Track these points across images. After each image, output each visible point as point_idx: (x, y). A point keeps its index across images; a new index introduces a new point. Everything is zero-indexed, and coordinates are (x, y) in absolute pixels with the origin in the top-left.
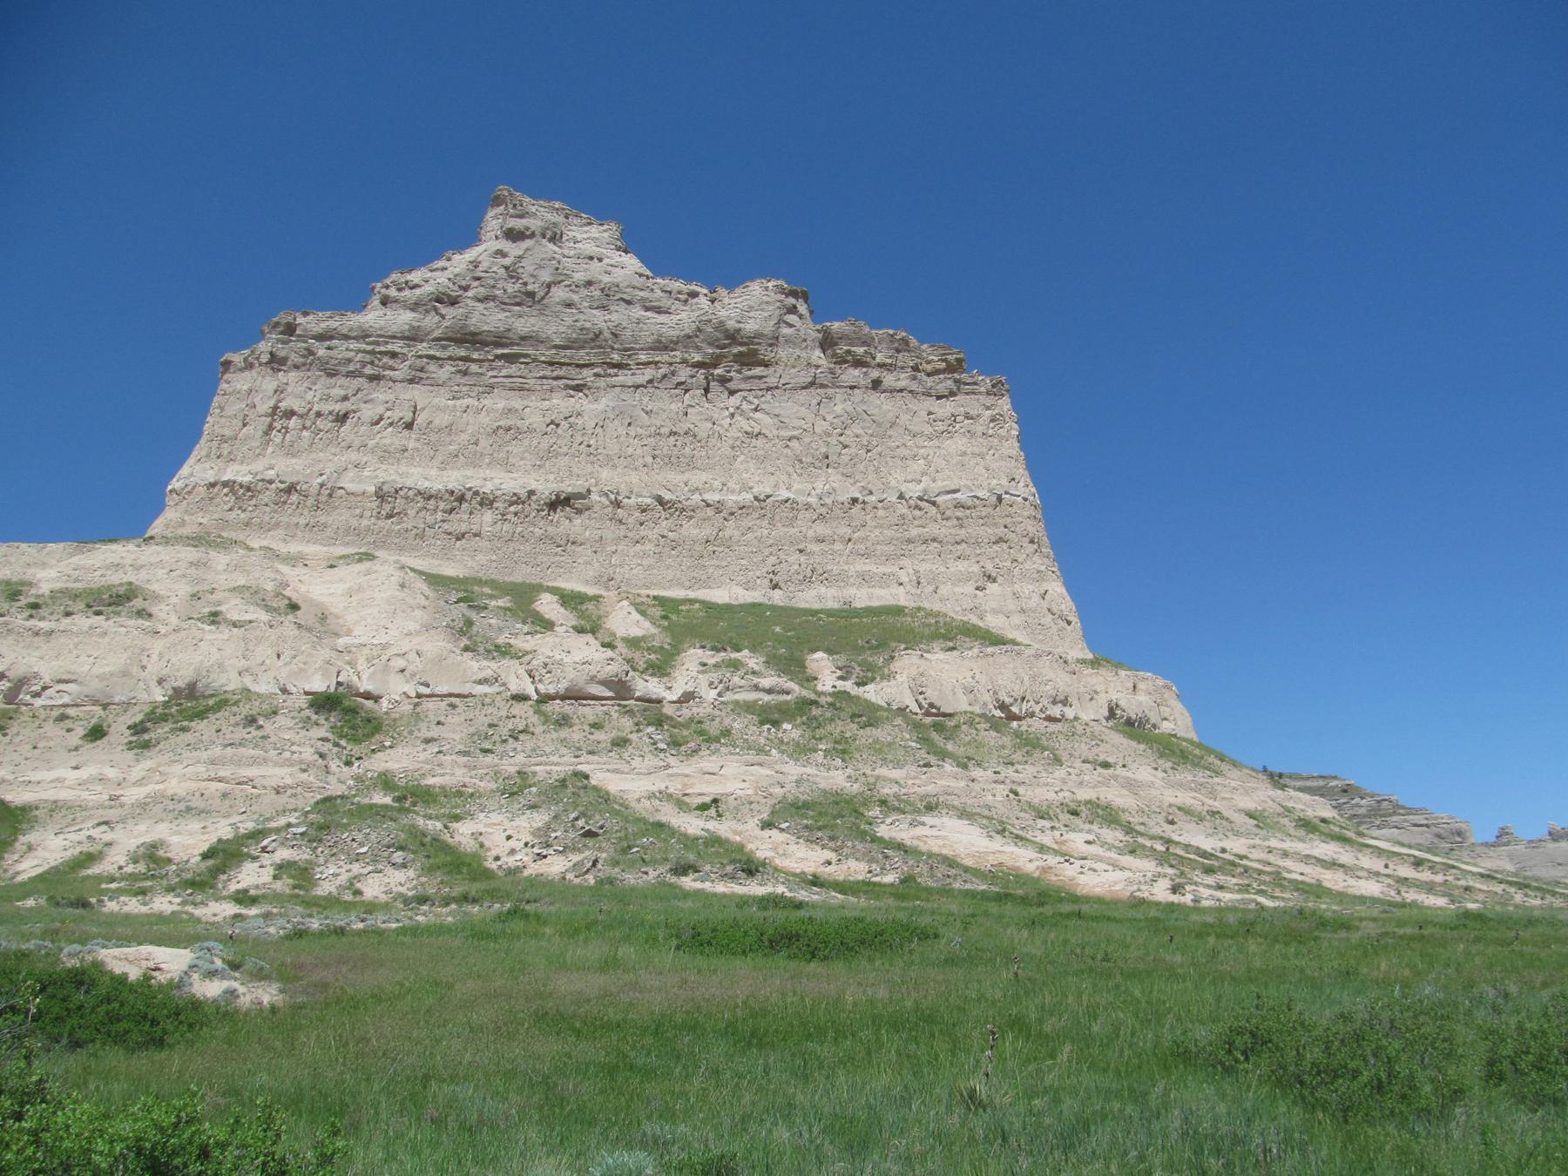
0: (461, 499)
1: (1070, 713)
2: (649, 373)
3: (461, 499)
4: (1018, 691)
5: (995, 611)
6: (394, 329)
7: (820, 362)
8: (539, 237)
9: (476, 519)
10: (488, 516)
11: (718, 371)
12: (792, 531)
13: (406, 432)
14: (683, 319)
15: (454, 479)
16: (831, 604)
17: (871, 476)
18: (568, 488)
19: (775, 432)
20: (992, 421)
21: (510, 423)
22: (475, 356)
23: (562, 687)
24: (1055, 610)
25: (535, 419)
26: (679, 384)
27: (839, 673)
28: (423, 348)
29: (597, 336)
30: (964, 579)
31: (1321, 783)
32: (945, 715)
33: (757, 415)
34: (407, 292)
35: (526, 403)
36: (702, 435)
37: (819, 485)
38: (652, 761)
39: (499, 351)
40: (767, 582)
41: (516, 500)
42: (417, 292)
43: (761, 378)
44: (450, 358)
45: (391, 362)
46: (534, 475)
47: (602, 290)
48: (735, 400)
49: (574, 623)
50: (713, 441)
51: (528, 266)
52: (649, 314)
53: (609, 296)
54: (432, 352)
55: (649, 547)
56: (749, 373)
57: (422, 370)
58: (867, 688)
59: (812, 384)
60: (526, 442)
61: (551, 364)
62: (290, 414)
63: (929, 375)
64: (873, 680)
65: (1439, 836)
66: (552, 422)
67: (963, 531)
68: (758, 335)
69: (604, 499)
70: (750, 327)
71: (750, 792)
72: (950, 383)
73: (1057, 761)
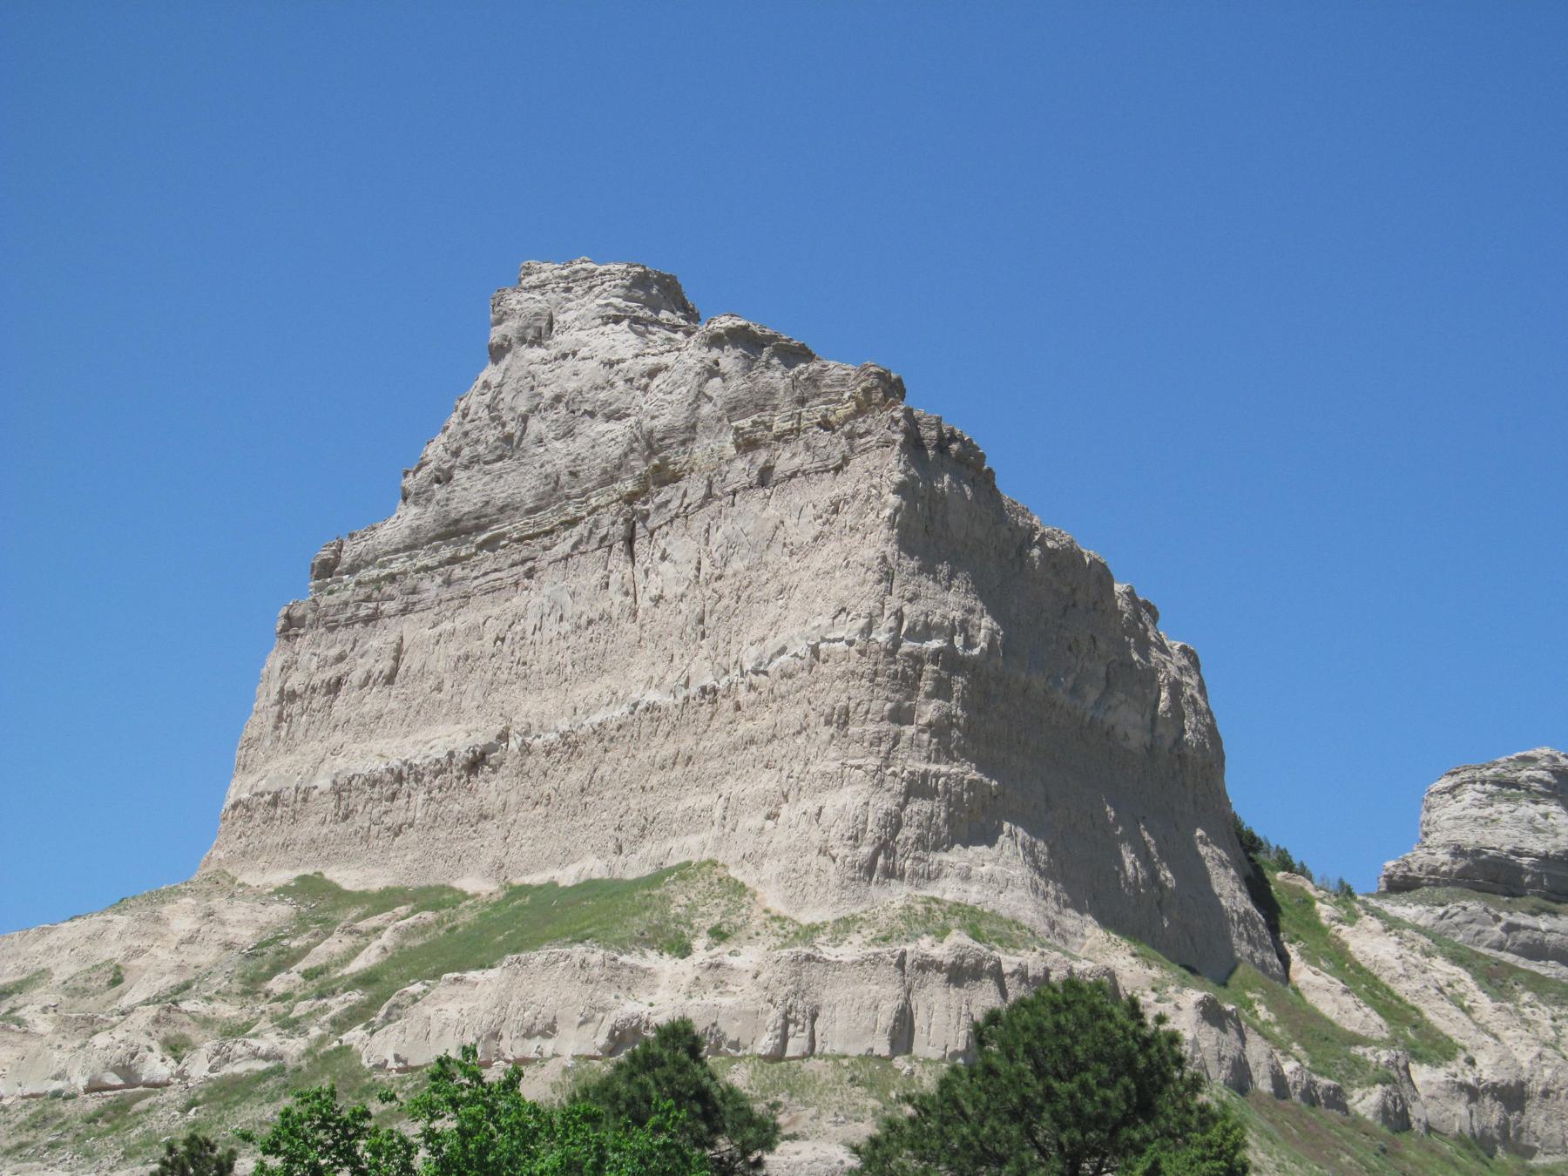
0: (400, 779)
3: (400, 779)
16: (647, 870)
25: (489, 637)
28: (423, 559)
36: (615, 612)
44: (441, 565)
51: (507, 394)
53: (573, 410)
55: (540, 809)
57: (414, 591)
62: (292, 696)
68: (670, 431)
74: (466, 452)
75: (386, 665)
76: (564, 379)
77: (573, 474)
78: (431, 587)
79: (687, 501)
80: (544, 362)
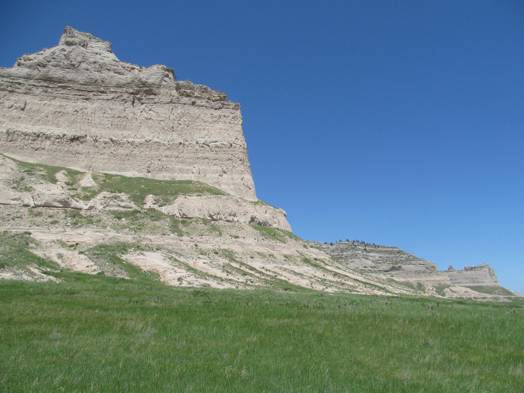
0: (38, 136)
1: (236, 219)
2: (113, 95)
3: (38, 136)
4: (217, 210)
5: (225, 184)
6: (21, 74)
7: (175, 95)
8: (78, 45)
9: (43, 143)
10: (48, 143)
11: (138, 96)
12: (157, 153)
13: (21, 112)
14: (128, 77)
15: (37, 129)
16: (168, 179)
17: (188, 135)
18: (78, 134)
19: (156, 118)
20: (233, 118)
21: (60, 110)
22: (51, 86)
23: (43, 203)
24: (245, 184)
25: (70, 109)
26: (124, 100)
27: (154, 202)
28: (31, 82)
29: (96, 81)
30: (215, 172)
31: (391, 249)
32: (189, 218)
33: (150, 112)
34: (27, 62)
35: (68, 103)
36: (130, 118)
37: (169, 137)
38: (61, 229)
39: (60, 85)
40: (146, 170)
41: (59, 137)
42: (31, 62)
43: (153, 99)
44: (41, 86)
45: (18, 86)
46: (67, 129)
47: (100, 65)
48: (143, 106)
49: (67, 181)
50: (133, 120)
51: (73, 55)
52: (116, 74)
53: (102, 67)
54: (34, 84)
55: (106, 156)
56: (149, 97)
57: (30, 90)
58: (162, 207)
59: (171, 102)
60: (66, 117)
61: (78, 90)
63: (213, 101)
64: (165, 205)
65: (427, 268)
66: (76, 111)
67: (217, 156)
68: (153, 84)
69: (91, 139)
70: (151, 81)
71: (92, 241)
72: (220, 104)
73: (221, 234)
77: (103, 81)
79: (160, 101)
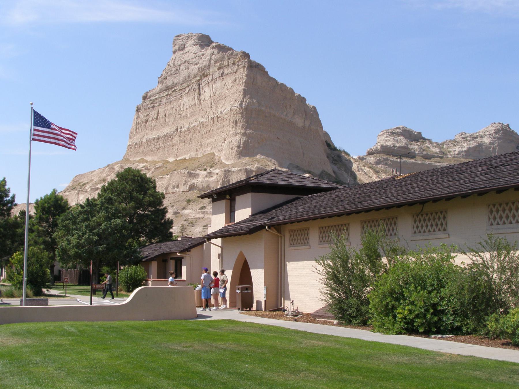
51: (176, 61)
68: (205, 66)
74: (169, 73)
75: (156, 116)
76: (186, 57)
78: (164, 100)
80: (183, 54)
